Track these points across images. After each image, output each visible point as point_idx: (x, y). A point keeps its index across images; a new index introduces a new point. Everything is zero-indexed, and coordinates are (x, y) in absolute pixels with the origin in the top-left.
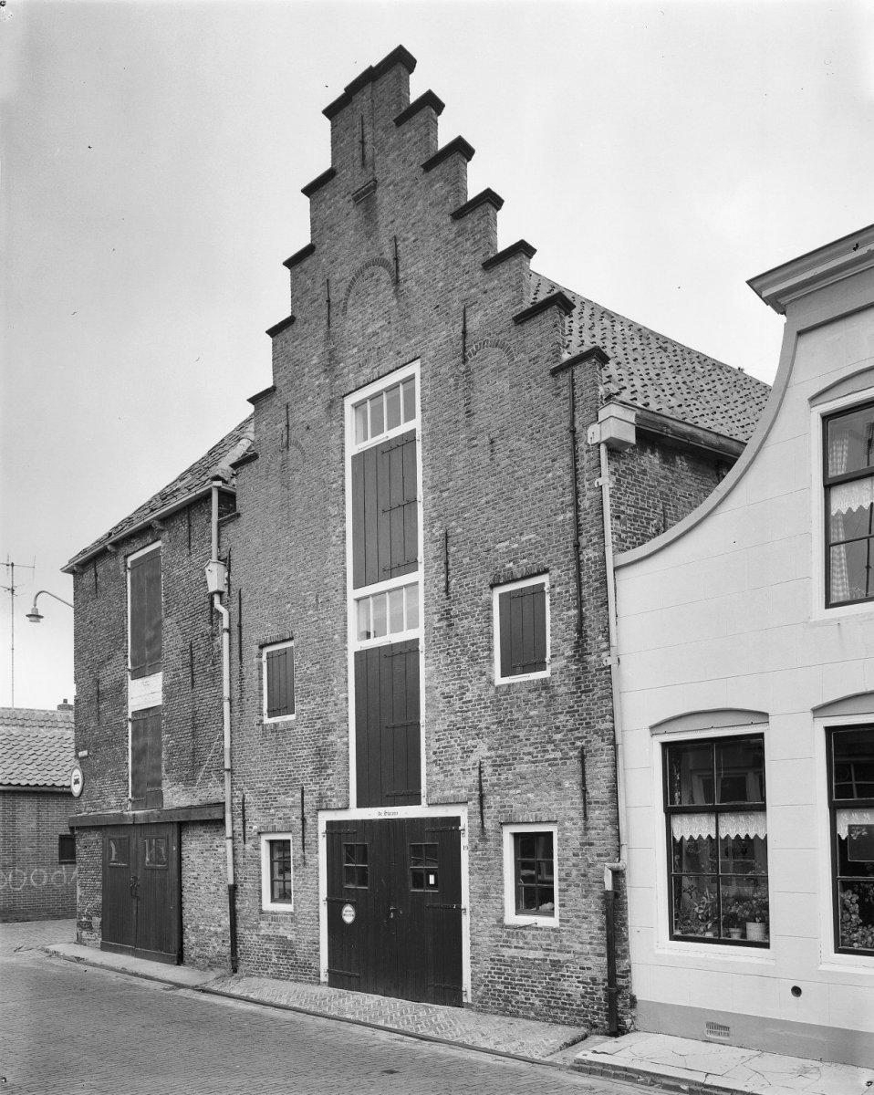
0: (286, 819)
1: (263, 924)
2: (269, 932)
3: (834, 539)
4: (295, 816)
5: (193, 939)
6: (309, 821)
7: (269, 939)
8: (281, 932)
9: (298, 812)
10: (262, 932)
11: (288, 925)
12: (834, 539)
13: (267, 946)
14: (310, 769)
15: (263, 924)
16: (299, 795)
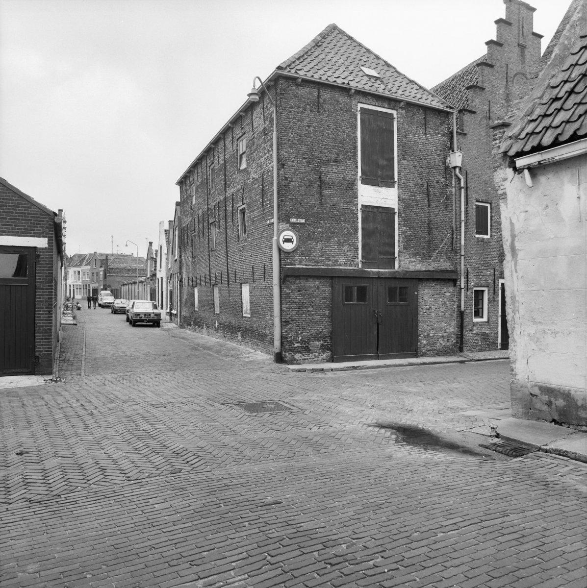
0: (487, 281)
1: (475, 328)
2: (478, 331)
3: (197, 578)
4: (490, 280)
5: (424, 342)
6: (496, 282)
7: (477, 334)
8: (483, 330)
9: (492, 278)
10: (474, 332)
11: (487, 327)
12: (197, 578)
13: (476, 338)
14: (497, 261)
15: (475, 328)
16: (492, 271)
